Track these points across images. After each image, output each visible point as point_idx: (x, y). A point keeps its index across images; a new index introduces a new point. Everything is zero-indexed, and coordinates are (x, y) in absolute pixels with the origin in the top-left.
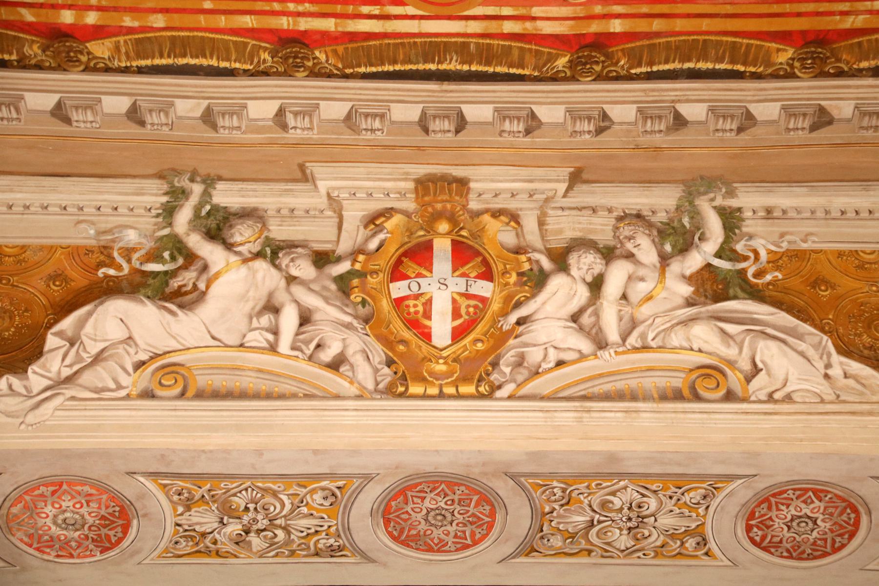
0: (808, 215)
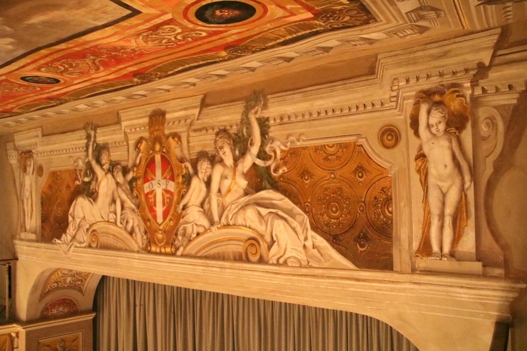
0: (300, 118)
